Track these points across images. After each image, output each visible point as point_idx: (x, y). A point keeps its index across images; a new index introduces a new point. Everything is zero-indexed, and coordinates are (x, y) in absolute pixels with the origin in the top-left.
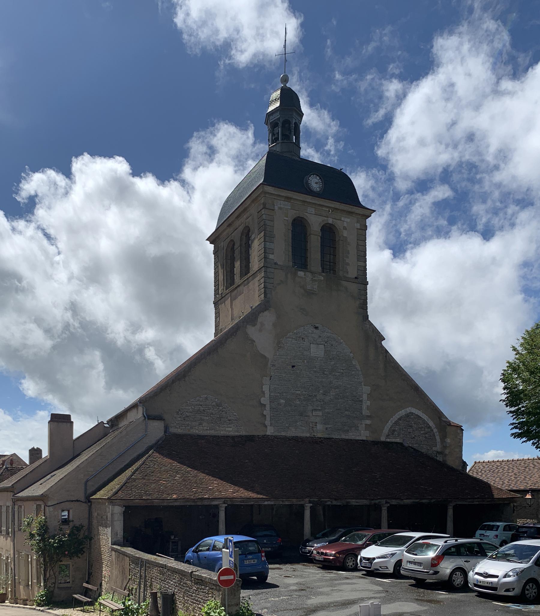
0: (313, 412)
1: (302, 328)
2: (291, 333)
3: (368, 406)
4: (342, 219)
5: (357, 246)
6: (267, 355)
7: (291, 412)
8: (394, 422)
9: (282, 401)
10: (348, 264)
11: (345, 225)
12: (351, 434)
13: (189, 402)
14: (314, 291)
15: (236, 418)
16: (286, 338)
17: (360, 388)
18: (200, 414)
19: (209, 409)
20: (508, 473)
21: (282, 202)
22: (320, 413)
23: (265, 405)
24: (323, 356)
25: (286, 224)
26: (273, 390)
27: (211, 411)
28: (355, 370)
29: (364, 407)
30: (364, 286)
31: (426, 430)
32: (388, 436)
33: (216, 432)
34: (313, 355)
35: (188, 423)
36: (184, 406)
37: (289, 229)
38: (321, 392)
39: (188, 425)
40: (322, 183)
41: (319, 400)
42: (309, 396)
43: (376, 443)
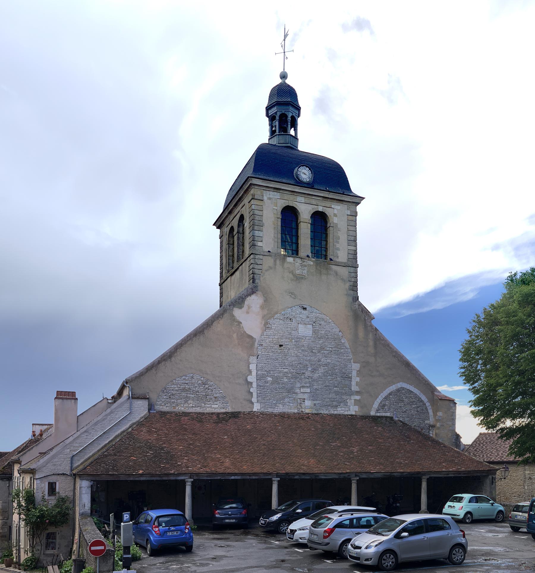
0: (301, 389)
1: (290, 309)
5: (347, 232)
6: (254, 336)
7: (278, 390)
8: (384, 397)
9: (269, 379)
10: (338, 249)
11: (336, 212)
12: (339, 409)
16: (274, 319)
17: (349, 365)
20: (505, 444)
21: (271, 192)
22: (308, 390)
23: (251, 383)
24: (311, 335)
25: (275, 213)
26: (259, 368)
28: (344, 348)
29: (353, 383)
30: (354, 268)
32: (377, 411)
34: (301, 334)
37: (278, 218)
38: (309, 369)
39: (173, 403)
40: (312, 174)
41: (308, 377)
43: (366, 418)
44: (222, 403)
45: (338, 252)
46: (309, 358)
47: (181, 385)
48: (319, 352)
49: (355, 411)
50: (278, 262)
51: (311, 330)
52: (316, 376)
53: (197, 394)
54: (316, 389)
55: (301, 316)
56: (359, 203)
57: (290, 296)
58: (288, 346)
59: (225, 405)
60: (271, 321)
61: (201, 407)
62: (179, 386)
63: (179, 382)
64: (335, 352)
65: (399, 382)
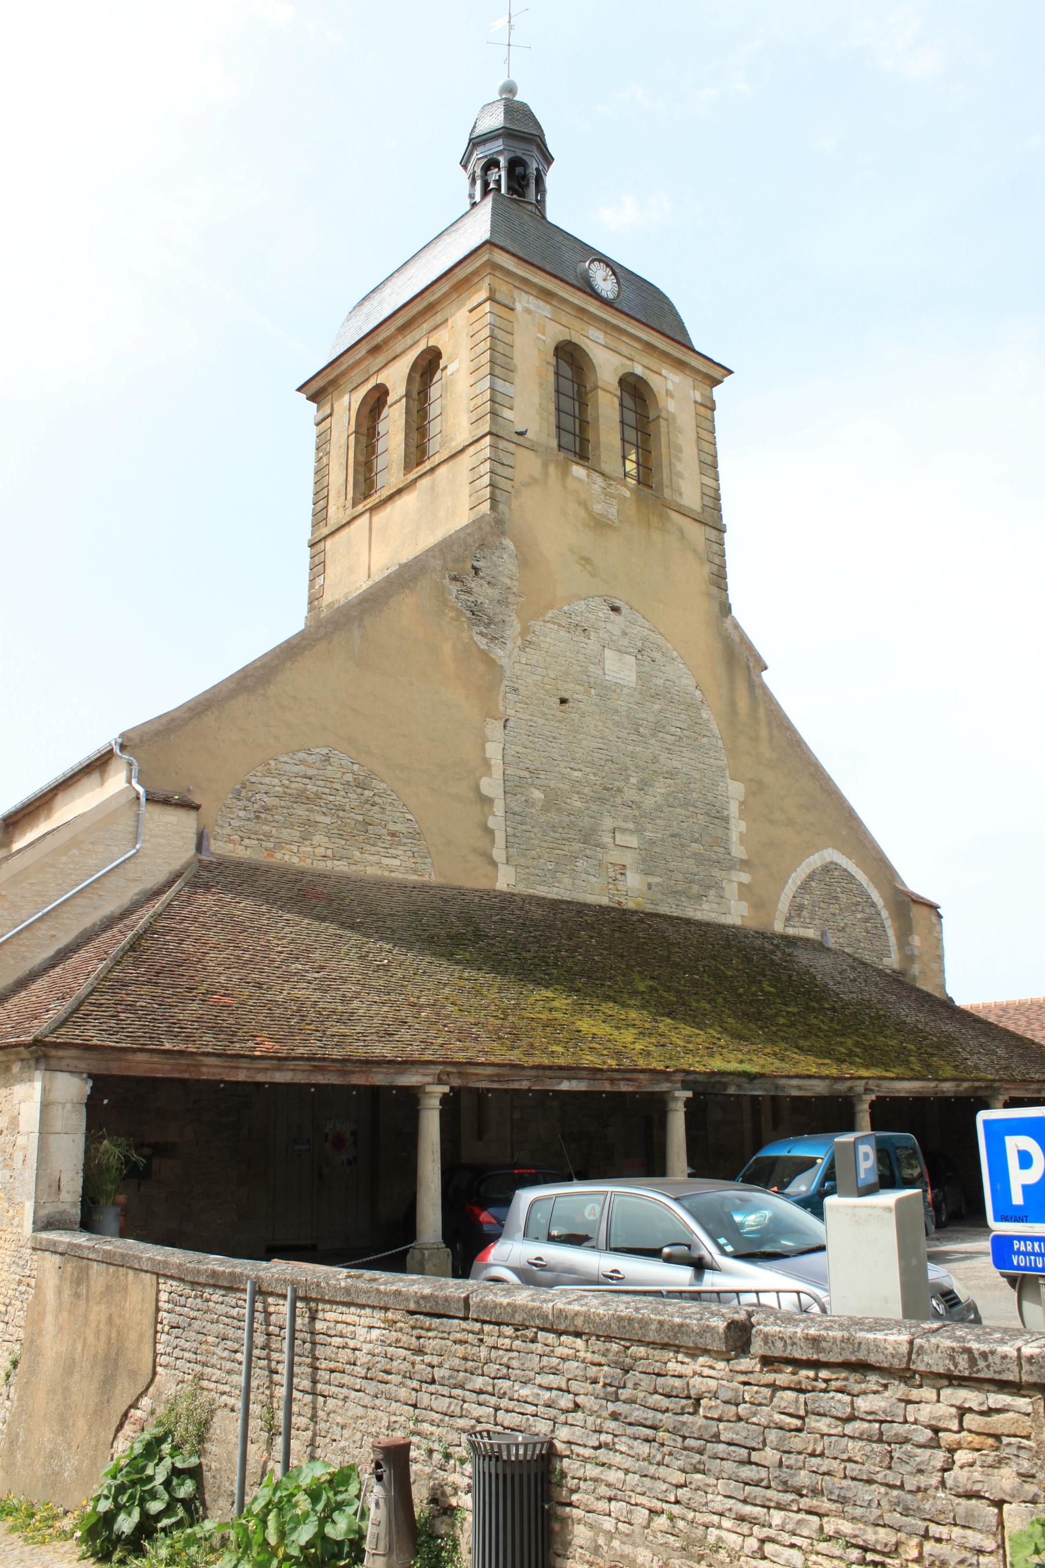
0: (617, 834)
2: (555, 611)
3: (741, 833)
4: (664, 372)
7: (560, 830)
8: (799, 883)
9: (538, 795)
10: (680, 475)
11: (670, 387)
12: (706, 906)
13: (272, 762)
14: (610, 519)
15: (411, 830)
16: (545, 622)
18: (307, 806)
19: (334, 792)
22: (633, 841)
24: (634, 685)
26: (511, 758)
27: (338, 798)
29: (734, 837)
31: (867, 911)
33: (353, 867)
35: (266, 828)
36: (258, 774)
38: (634, 780)
39: (268, 836)
41: (630, 804)
42: (605, 789)
44: (410, 854)
45: (682, 483)
46: (630, 748)
47: (293, 779)
48: (653, 735)
49: (742, 916)
50: (552, 470)
51: (634, 669)
52: (649, 802)
53: (338, 817)
54: (652, 842)
55: (609, 626)
56: (718, 382)
57: (582, 565)
58: (581, 705)
59: (419, 860)
60: (537, 626)
61: (350, 861)
62: (287, 782)
63: (287, 767)
64: (689, 741)
65: (826, 847)
